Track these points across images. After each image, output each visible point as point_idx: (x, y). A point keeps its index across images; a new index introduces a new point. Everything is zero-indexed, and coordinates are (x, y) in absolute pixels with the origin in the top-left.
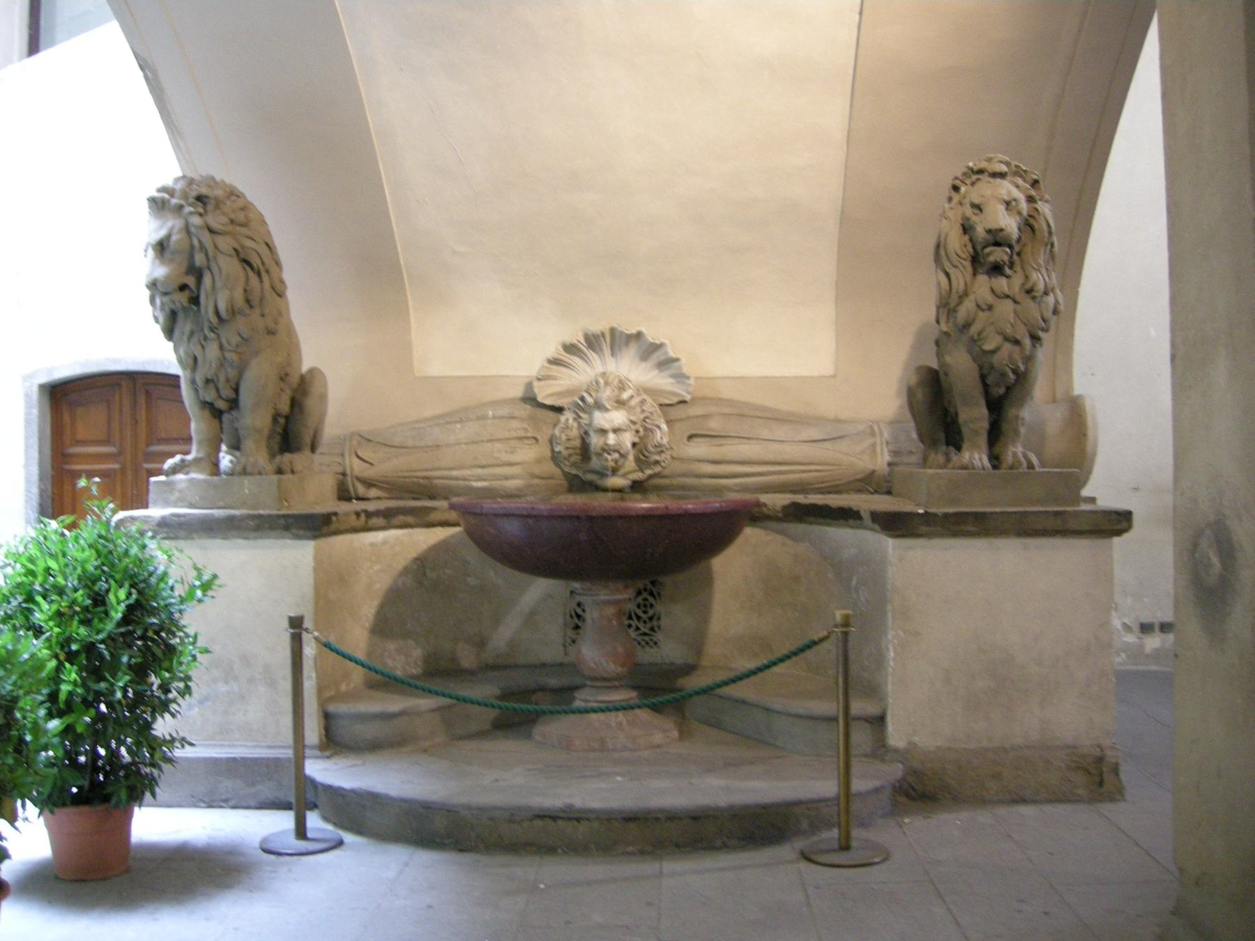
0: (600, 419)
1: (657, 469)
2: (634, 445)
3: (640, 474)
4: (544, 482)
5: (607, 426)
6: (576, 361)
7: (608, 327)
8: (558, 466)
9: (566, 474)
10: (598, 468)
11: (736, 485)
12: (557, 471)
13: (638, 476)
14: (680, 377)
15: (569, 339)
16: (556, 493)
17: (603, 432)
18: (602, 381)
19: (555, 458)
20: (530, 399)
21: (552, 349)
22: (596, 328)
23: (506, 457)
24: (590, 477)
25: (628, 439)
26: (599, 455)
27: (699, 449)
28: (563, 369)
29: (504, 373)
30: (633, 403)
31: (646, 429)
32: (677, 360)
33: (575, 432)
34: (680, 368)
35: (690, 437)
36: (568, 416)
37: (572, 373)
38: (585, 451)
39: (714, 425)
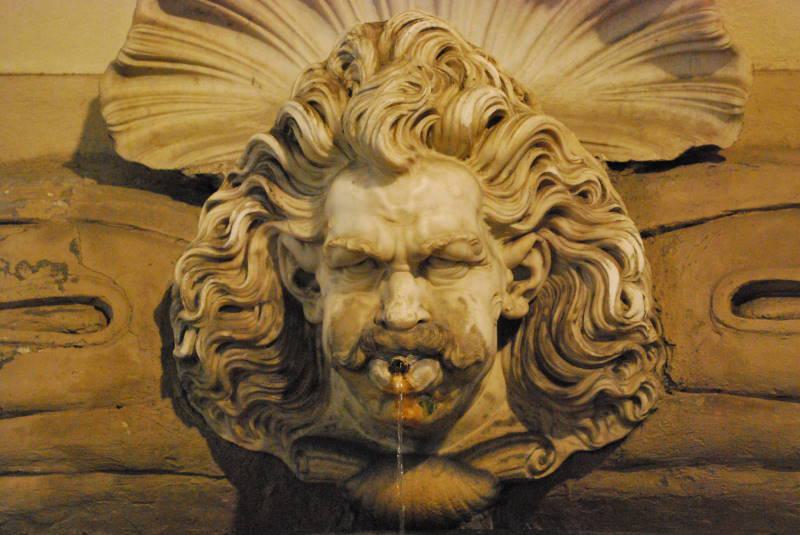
0: (358, 213)
1: (608, 431)
2: (507, 327)
3: (535, 453)
5: (387, 241)
9: (226, 455)
12: (195, 439)
17: (371, 267)
19: (179, 381)
24: (322, 466)
25: (478, 301)
28: (229, 38)
30: (501, 143)
33: (256, 278)
35: (744, 297)
36: (233, 209)
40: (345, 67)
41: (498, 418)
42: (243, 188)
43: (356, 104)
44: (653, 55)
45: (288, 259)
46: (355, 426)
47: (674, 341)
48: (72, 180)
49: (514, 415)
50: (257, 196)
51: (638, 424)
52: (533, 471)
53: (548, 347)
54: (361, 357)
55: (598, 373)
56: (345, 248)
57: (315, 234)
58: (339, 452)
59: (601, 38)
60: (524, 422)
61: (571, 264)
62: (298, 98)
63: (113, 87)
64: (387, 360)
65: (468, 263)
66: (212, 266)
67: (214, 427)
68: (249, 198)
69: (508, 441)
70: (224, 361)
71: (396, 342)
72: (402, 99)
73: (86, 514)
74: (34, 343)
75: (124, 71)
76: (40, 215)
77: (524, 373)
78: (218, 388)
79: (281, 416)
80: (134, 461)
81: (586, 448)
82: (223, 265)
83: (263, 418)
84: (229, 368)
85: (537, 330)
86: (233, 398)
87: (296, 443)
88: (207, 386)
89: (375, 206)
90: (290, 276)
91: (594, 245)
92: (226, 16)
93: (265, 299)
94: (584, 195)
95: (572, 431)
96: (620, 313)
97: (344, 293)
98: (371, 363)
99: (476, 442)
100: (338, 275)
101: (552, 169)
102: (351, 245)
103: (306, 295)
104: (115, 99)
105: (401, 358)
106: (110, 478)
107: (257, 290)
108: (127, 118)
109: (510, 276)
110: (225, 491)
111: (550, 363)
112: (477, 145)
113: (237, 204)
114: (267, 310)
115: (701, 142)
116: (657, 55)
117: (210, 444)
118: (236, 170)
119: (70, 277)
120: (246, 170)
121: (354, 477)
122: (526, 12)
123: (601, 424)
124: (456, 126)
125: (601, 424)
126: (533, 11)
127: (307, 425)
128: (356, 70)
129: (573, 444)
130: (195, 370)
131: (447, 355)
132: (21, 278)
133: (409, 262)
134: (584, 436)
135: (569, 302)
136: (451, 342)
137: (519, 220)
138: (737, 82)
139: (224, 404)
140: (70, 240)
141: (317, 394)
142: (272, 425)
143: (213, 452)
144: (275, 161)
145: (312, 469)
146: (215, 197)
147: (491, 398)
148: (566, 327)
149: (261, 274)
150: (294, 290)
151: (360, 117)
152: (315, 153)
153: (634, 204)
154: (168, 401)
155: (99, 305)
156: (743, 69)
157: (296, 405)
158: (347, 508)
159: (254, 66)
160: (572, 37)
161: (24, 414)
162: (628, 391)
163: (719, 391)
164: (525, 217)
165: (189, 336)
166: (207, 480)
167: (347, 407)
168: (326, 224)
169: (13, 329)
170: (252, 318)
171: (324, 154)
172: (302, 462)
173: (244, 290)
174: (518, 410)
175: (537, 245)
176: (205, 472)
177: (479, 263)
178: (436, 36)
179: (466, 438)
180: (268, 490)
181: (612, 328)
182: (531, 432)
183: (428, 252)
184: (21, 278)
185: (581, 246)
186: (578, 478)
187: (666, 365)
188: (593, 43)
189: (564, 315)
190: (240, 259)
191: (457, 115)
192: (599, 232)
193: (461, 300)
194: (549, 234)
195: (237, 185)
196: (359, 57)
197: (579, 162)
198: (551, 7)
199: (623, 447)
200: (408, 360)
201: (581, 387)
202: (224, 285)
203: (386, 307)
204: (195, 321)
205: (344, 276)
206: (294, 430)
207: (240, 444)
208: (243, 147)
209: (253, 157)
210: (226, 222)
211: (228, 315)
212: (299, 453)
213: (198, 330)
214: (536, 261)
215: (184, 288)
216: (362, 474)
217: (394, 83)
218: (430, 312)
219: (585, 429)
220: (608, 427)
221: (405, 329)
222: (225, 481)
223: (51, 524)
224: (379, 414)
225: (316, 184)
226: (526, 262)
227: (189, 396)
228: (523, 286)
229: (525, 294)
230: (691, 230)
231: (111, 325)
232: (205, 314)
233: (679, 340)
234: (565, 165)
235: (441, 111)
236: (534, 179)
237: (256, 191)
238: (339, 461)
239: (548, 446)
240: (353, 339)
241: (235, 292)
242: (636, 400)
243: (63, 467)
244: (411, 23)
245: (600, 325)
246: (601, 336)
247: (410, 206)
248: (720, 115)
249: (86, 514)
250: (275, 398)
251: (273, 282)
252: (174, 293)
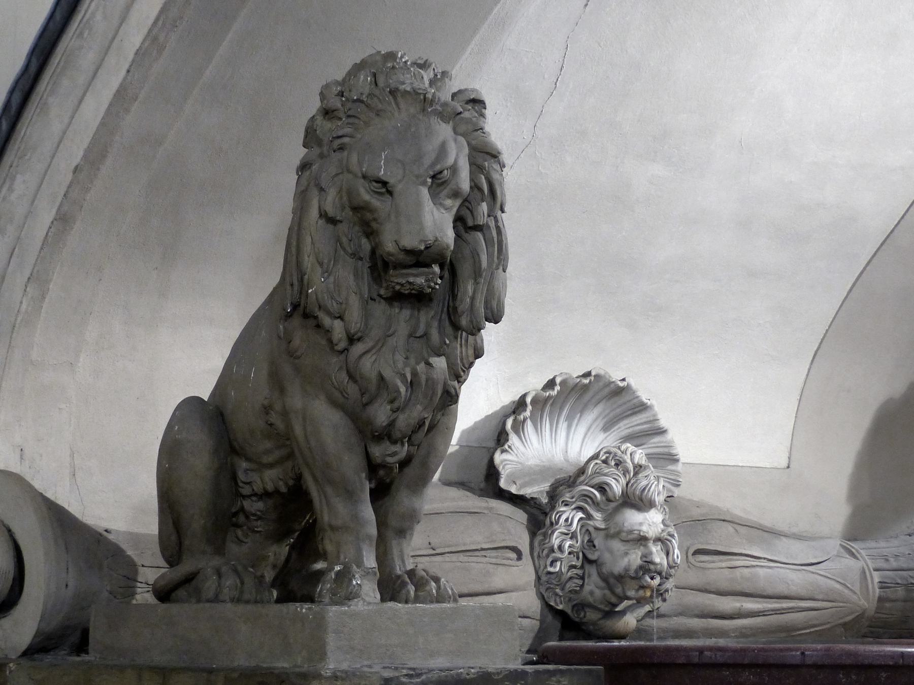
42: (573, 507)
46: (591, 600)
70: (569, 574)
121: (600, 619)
167: (592, 593)
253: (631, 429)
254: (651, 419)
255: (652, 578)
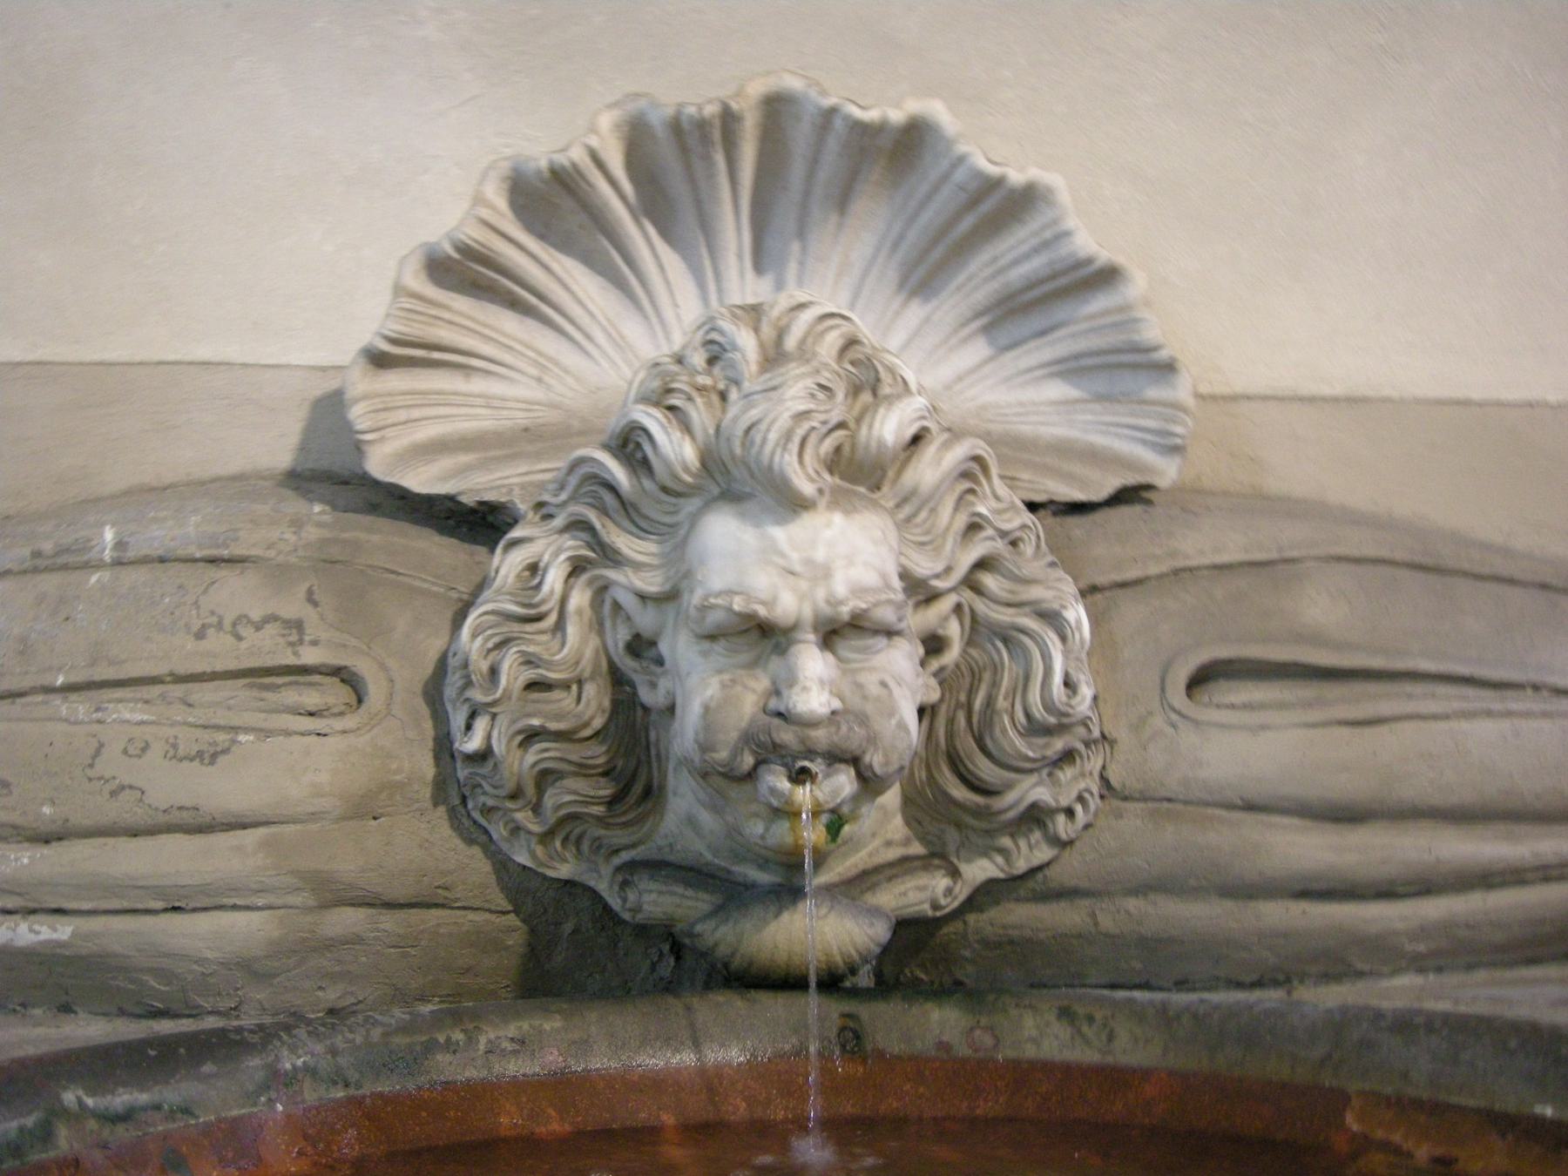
0: (742, 559)
1: (1030, 852)
3: (941, 882)
4: (389, 922)
5: (787, 604)
6: (572, 281)
7: (757, 88)
8: (473, 833)
9: (520, 886)
10: (697, 848)
11: (1423, 931)
12: (478, 865)
13: (926, 892)
14: (1132, 365)
15: (543, 145)
16: (464, 1006)
17: (763, 636)
18: (746, 343)
19: (458, 784)
20: (334, 476)
21: (456, 198)
22: (687, 87)
23: (171, 785)
24: (656, 901)
25: (898, 681)
26: (730, 778)
27: (1251, 743)
28: (509, 322)
29: (203, 352)
30: (929, 469)
31: (977, 629)
32: (1108, 276)
33: (577, 645)
34: (1125, 318)
35: (1200, 680)
36: (540, 550)
37: (546, 341)
38: (630, 746)
39: (1324, 613)
40: (712, 361)
41: (889, 836)
42: (559, 522)
43: (744, 411)
44: (1073, 364)
45: (619, 621)
47: (1115, 735)
48: (295, 505)
49: (910, 833)
50: (583, 535)
51: (1071, 843)
52: (935, 906)
53: (966, 744)
54: (748, 760)
55: (1034, 778)
56: (729, 610)
57: (667, 587)
58: (688, 884)
59: (991, 342)
60: (923, 839)
61: (995, 634)
62: (645, 399)
63: (362, 383)
64: (785, 765)
65: (890, 633)
66: (516, 627)
67: (505, 846)
68: (566, 536)
69: (903, 866)
70: (531, 758)
71: (803, 741)
72: (812, 406)
73: (325, 963)
74: (261, 730)
75: (379, 360)
76: (253, 552)
77: (930, 776)
78: (513, 797)
79: (602, 832)
80: (399, 892)
81: (1001, 875)
82: (529, 627)
83: (573, 837)
84: (537, 769)
85: (951, 721)
86: (536, 809)
87: (618, 869)
88: (502, 792)
89: (771, 550)
90: (621, 645)
91: (1027, 609)
92: (510, 292)
93: (586, 674)
94: (1014, 543)
95: (985, 853)
96: (1064, 699)
97: (720, 672)
98: (763, 768)
99: (861, 867)
100: (706, 645)
101: (982, 509)
102: (738, 605)
103: (646, 671)
104: (365, 397)
105: (806, 763)
106: (361, 914)
107: (577, 663)
108: (381, 423)
109: (921, 651)
110: (513, 931)
111: (970, 766)
112: (891, 474)
113: (549, 545)
114: (590, 690)
115: (1131, 479)
116: (1070, 368)
117: (497, 871)
118: (546, 497)
119: (307, 638)
120: (563, 497)
122: (896, 304)
123: (1022, 843)
124: (874, 444)
125: (1022, 843)
126: (905, 304)
127: (633, 846)
128: (732, 365)
129: (984, 870)
130: (486, 769)
131: (867, 759)
132: (239, 638)
133: (816, 629)
134: (1000, 859)
135: (995, 684)
136: (872, 739)
137: (937, 576)
138: (1177, 406)
139: (523, 817)
140: (307, 585)
141: (650, 805)
142: (585, 846)
143: (499, 880)
144: (612, 488)
145: (645, 907)
146: (516, 533)
147: (886, 814)
148: (996, 719)
149: (584, 641)
150: (628, 664)
151: (748, 430)
152: (676, 477)
153: (1064, 557)
154: (442, 810)
155: (345, 677)
156: (1182, 390)
157: (623, 819)
158: (666, 948)
159: (541, 360)
160: (954, 341)
161: (244, 826)
162: (1064, 802)
163: (1169, 800)
164: (948, 570)
165: (481, 724)
166: (487, 916)
167: (691, 821)
168: (688, 575)
169: (229, 708)
170: (567, 702)
171: (689, 479)
172: (632, 896)
173: (559, 663)
174: (915, 824)
175: (958, 609)
176: (487, 906)
177: (898, 633)
178: (837, 326)
179: (848, 863)
180: (568, 927)
181: (1052, 720)
182: (933, 855)
183: (846, 617)
184: (239, 638)
185: (1011, 611)
186: (982, 911)
187: (1104, 767)
188: (979, 349)
189: (990, 702)
190: (551, 620)
191: (875, 432)
192: (1035, 593)
193: (884, 684)
194: (967, 596)
195: (550, 516)
196: (735, 348)
197: (1000, 503)
198: (927, 300)
199: (1047, 872)
200: (816, 766)
201: (1010, 797)
202: (533, 654)
203: (785, 693)
204: (494, 703)
205: (719, 647)
206: (617, 851)
207: (540, 870)
208: (561, 463)
209: (573, 481)
210: (533, 568)
211: (535, 695)
212: (625, 884)
213: (494, 716)
214: (954, 630)
215: (474, 656)
216: (718, 911)
217: (800, 385)
218: (842, 699)
219: (1002, 851)
220: (1030, 847)
221: (811, 723)
222: (512, 916)
223: (275, 976)
224: (762, 837)
225: (667, 519)
226: (940, 632)
227: (470, 805)
228: (935, 664)
229: (935, 675)
230: (1129, 592)
231: (364, 707)
232: (507, 695)
233: (1120, 733)
234: (994, 504)
235: (852, 425)
236: (962, 520)
237: (578, 525)
238: (683, 896)
239: (955, 873)
240: (734, 735)
241: (549, 665)
242: (1070, 813)
243: (296, 900)
244: (802, 306)
245: (1038, 715)
246: (1035, 729)
247: (820, 555)
248: (1154, 446)
249: (325, 963)
250: (598, 810)
251: (597, 652)
252: (453, 662)
253: (1001, 280)
254: (1048, 234)
255: (800, 776)
